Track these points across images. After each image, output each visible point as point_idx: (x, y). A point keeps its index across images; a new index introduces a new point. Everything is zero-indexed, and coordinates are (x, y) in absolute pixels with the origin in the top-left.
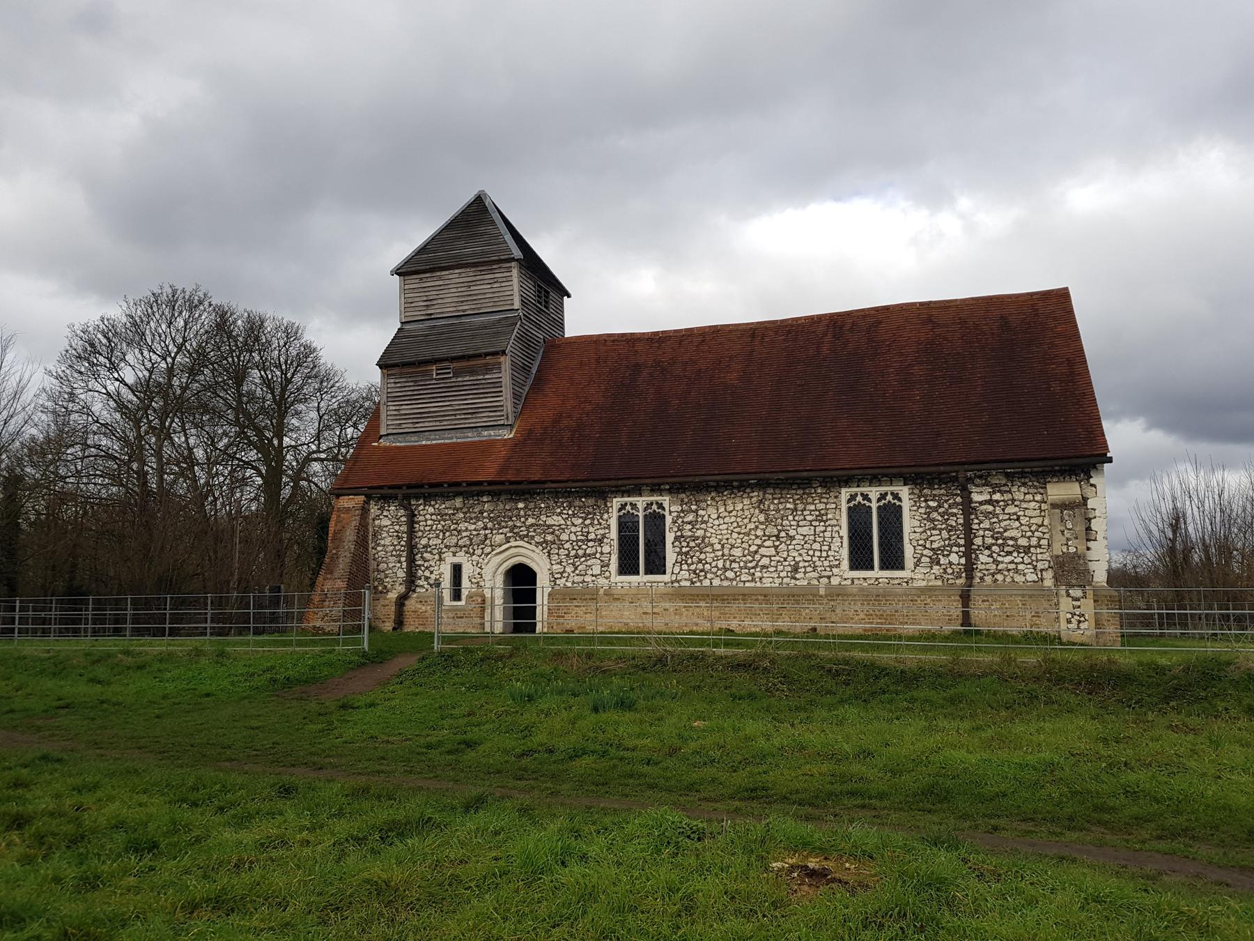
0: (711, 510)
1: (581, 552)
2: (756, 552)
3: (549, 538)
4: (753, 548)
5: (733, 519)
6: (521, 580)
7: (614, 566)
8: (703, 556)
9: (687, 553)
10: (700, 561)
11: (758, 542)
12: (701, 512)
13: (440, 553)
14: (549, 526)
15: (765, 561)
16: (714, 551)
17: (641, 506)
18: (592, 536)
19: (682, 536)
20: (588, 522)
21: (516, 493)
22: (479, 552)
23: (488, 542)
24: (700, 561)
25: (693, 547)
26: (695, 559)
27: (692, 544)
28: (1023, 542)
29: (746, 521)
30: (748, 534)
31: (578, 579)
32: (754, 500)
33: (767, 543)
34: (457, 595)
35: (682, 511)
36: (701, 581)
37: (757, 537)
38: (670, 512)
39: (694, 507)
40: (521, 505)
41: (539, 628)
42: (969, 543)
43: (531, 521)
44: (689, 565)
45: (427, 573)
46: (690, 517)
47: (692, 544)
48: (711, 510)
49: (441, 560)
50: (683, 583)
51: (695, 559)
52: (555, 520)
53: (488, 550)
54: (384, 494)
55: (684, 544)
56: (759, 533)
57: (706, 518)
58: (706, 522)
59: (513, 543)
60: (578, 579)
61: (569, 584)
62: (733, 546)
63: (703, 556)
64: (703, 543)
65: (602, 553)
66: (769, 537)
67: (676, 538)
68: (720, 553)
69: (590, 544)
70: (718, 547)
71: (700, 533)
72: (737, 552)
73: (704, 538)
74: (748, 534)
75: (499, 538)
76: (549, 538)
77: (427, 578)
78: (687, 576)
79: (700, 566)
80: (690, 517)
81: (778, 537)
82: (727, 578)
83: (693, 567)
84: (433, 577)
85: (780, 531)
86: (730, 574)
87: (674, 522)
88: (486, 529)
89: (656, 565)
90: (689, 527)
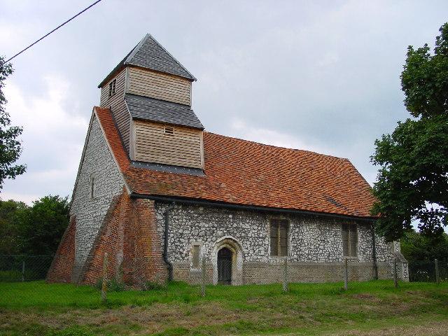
0: (304, 227)
1: (256, 243)
3: (243, 235)
4: (317, 245)
6: (226, 256)
7: (269, 252)
13: (189, 239)
14: (244, 229)
18: (261, 236)
20: (259, 228)
21: (228, 208)
22: (209, 240)
23: (214, 234)
31: (255, 257)
33: (322, 244)
34: (196, 265)
40: (231, 216)
41: (234, 284)
42: (374, 245)
43: (235, 225)
45: (181, 250)
48: (304, 227)
49: (189, 243)
52: (247, 226)
53: (214, 239)
54: (160, 200)
59: (228, 237)
60: (255, 257)
61: (251, 260)
65: (265, 245)
69: (260, 239)
70: (306, 244)
72: (312, 247)
75: (220, 233)
76: (243, 235)
77: (181, 253)
79: (301, 253)
84: (185, 252)
86: (310, 257)
88: (213, 227)
89: (285, 253)
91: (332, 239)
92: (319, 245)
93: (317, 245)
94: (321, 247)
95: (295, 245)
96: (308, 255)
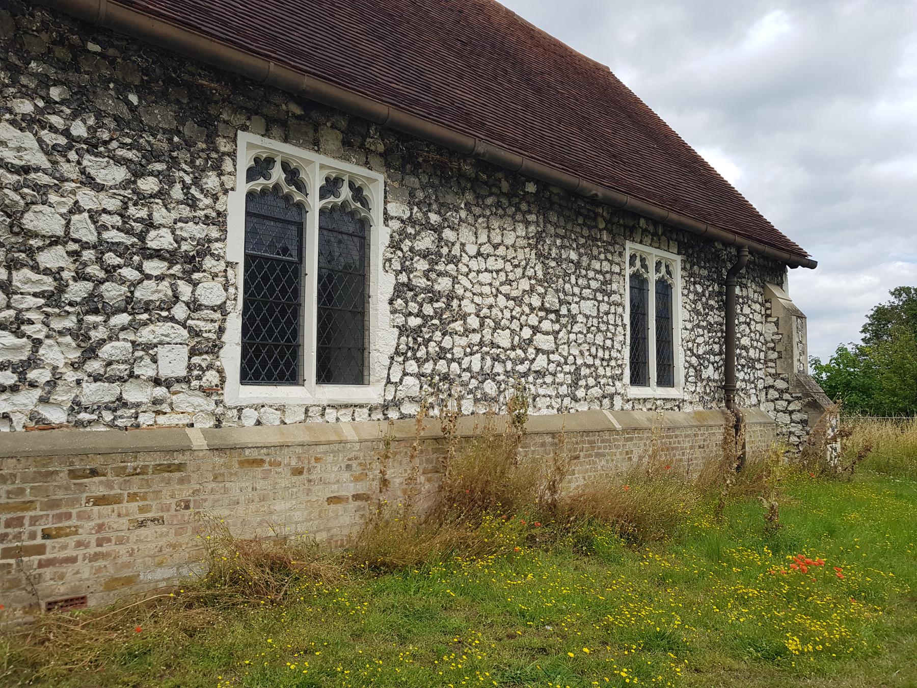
0: (466, 234)
2: (530, 341)
4: (527, 333)
5: (500, 264)
8: (447, 342)
9: (418, 330)
10: (442, 353)
11: (533, 320)
12: (448, 234)
15: (541, 362)
16: (467, 332)
17: (315, 180)
19: (409, 286)
24: (442, 353)
25: (431, 316)
26: (433, 347)
27: (428, 310)
28: (752, 353)
29: (519, 271)
30: (518, 301)
32: (532, 228)
33: (546, 325)
35: (411, 221)
36: (442, 403)
37: (532, 309)
38: (387, 217)
39: (434, 218)
44: (420, 362)
46: (426, 242)
47: (428, 310)
50: (409, 409)
51: (433, 347)
55: (413, 307)
56: (536, 302)
57: (456, 251)
58: (454, 260)
62: (497, 326)
63: (447, 342)
64: (447, 312)
66: (548, 311)
67: (400, 290)
68: (475, 338)
70: (473, 322)
71: (444, 284)
72: (503, 339)
73: (451, 297)
74: (518, 301)
78: (415, 391)
79: (442, 366)
80: (426, 242)
81: (556, 312)
82: (485, 397)
83: (428, 368)
85: (561, 302)
87: (395, 246)
90: (422, 265)
91: (588, 307)
92: (535, 330)
93: (527, 333)
94: (542, 341)
95: (414, 322)
96: (485, 376)
